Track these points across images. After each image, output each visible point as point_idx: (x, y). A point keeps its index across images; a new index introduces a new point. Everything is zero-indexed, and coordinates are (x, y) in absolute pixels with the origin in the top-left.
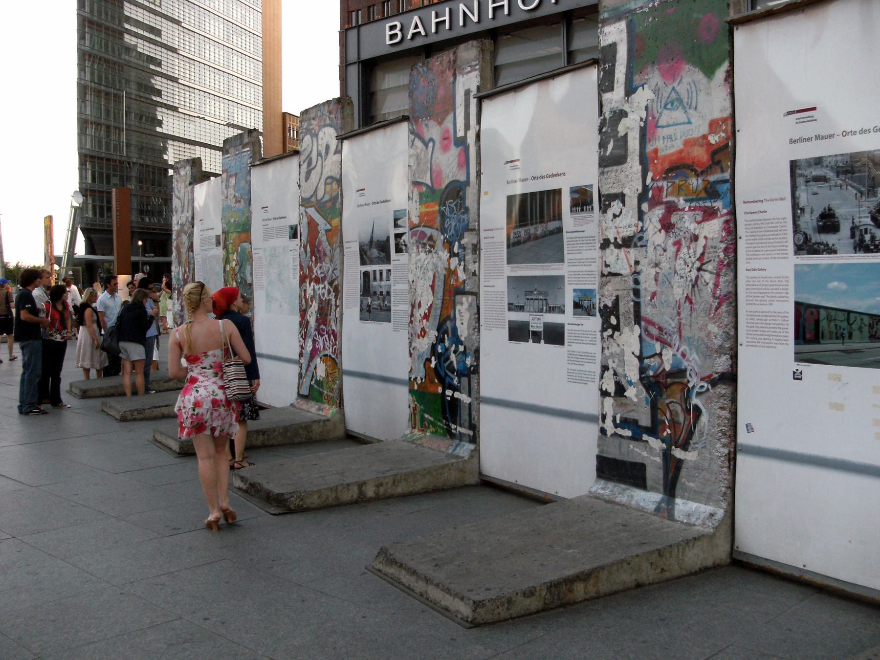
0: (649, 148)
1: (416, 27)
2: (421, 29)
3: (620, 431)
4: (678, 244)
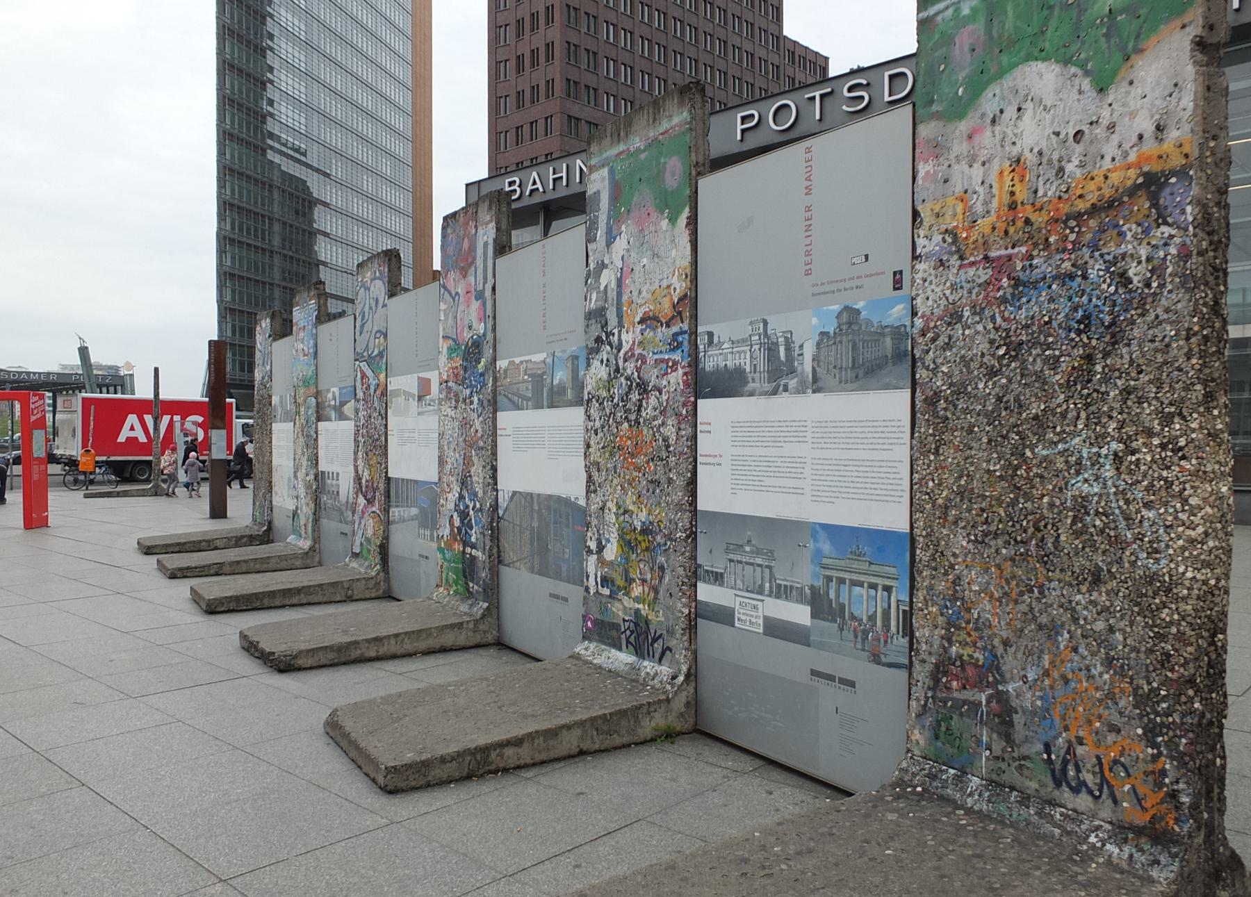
1: (534, 183)
2: (539, 185)
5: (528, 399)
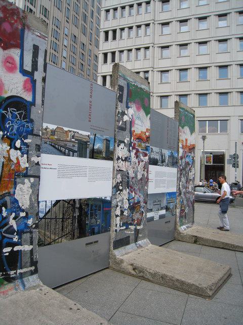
0: (132, 129)
3: (122, 228)
4: (139, 162)
5: (74, 152)
